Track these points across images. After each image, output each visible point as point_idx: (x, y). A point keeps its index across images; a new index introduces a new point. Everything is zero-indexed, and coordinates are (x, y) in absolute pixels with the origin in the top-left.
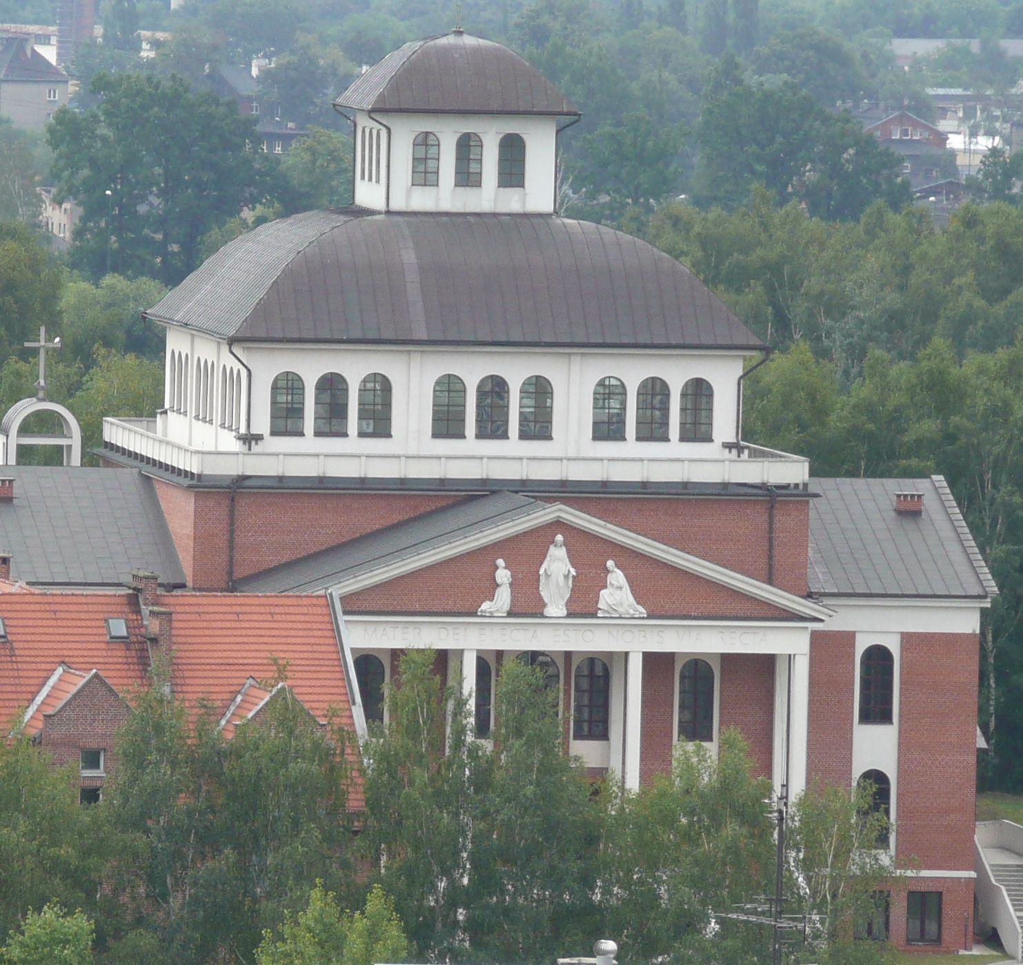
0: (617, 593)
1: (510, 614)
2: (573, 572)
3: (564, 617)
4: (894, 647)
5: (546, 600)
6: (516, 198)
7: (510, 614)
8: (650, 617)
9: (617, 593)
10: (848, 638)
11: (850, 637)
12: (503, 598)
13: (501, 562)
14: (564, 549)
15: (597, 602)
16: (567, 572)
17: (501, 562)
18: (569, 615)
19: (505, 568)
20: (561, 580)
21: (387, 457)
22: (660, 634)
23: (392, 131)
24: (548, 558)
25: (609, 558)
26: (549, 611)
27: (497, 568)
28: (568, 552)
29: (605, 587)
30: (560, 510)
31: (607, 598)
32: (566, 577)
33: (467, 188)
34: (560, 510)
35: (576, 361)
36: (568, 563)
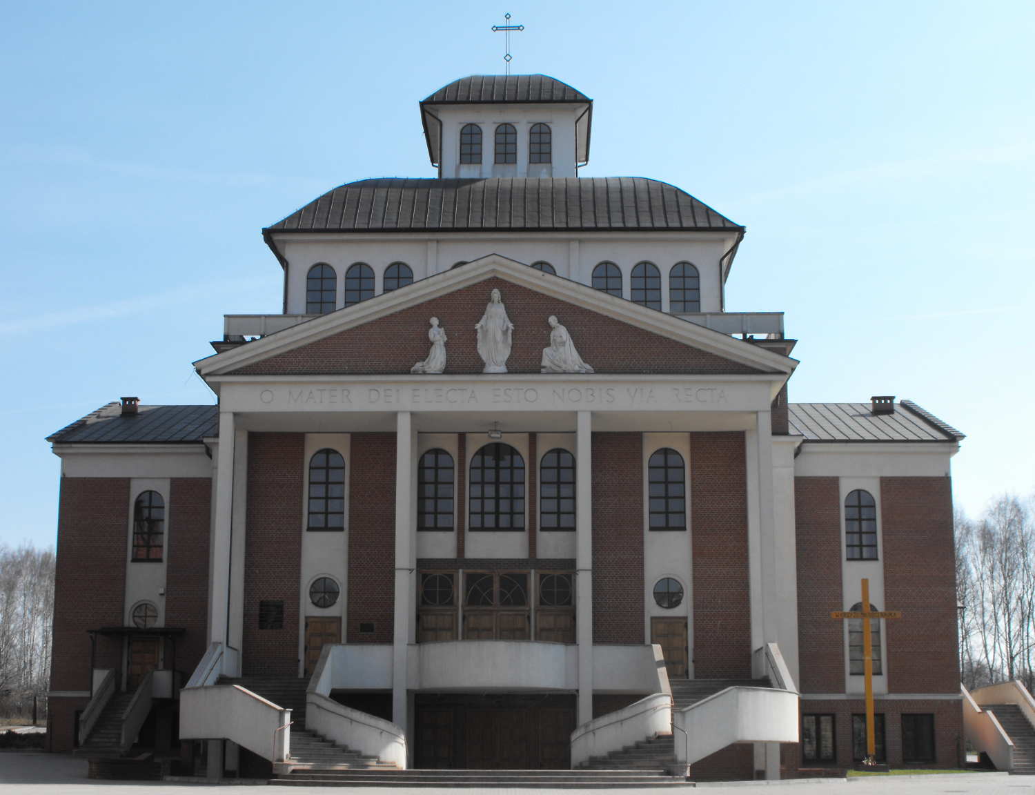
0: (562, 349)
1: (446, 372)
2: (511, 326)
3: (505, 373)
4: (875, 492)
5: (484, 358)
6: (545, 171)
7: (446, 372)
8: (597, 372)
9: (562, 349)
10: (832, 484)
11: (833, 483)
12: (438, 357)
13: (434, 321)
14: (502, 306)
15: (540, 360)
16: (505, 328)
17: (434, 321)
18: (510, 372)
19: (439, 326)
20: (499, 336)
21: (510, 433)
22: (610, 392)
23: (443, 124)
24: (485, 316)
25: (551, 314)
26: (490, 368)
27: (431, 326)
28: (507, 309)
29: (548, 345)
30: (494, 263)
31: (548, 356)
32: (505, 333)
33: (505, 165)
34: (494, 263)
35: (575, 246)
36: (507, 319)
